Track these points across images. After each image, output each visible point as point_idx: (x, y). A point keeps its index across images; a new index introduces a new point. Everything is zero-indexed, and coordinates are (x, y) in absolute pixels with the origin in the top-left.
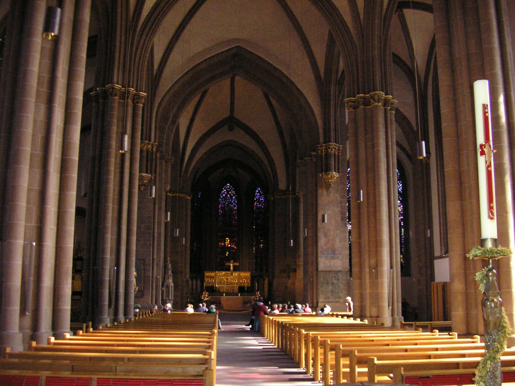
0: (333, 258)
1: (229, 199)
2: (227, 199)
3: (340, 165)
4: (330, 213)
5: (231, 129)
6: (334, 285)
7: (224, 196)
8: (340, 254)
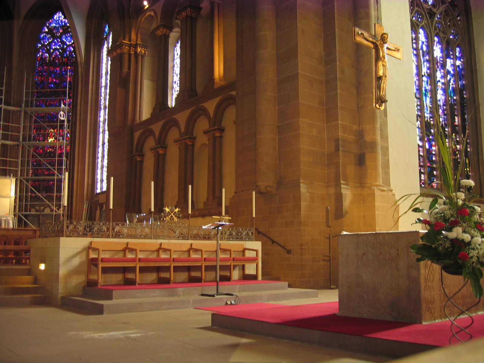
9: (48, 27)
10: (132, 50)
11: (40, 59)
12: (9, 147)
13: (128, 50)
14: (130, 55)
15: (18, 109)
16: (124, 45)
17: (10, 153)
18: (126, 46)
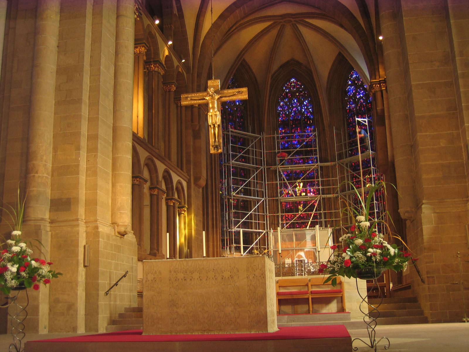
1: (297, 107)
2: (293, 107)
7: (286, 103)
9: (350, 80)
10: (382, 86)
11: (349, 111)
12: (332, 199)
13: (379, 88)
14: (381, 91)
15: (333, 163)
16: (374, 84)
17: (334, 205)
18: (376, 84)
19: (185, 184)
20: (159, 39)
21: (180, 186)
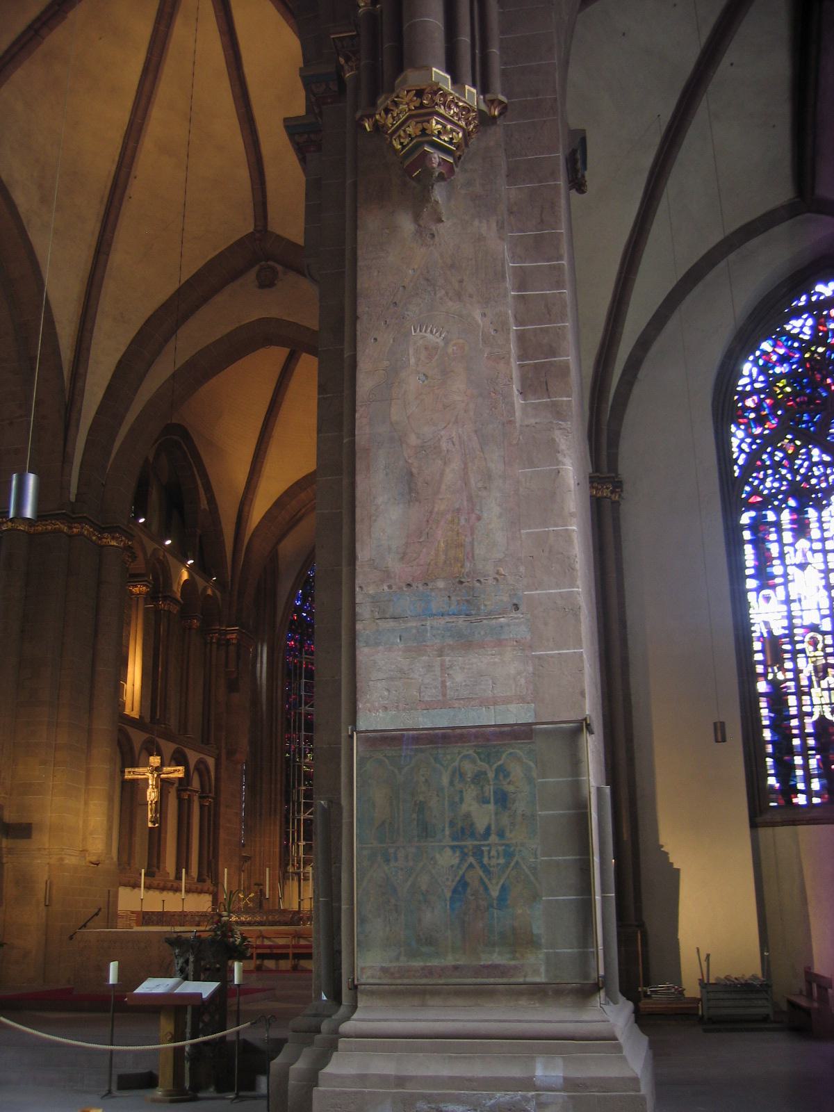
0: (466, 643)
3: (495, 50)
4: (435, 339)
5: (267, 283)
6: (470, 843)
8: (516, 607)
19: (211, 762)
20: (172, 561)
21: (202, 766)
